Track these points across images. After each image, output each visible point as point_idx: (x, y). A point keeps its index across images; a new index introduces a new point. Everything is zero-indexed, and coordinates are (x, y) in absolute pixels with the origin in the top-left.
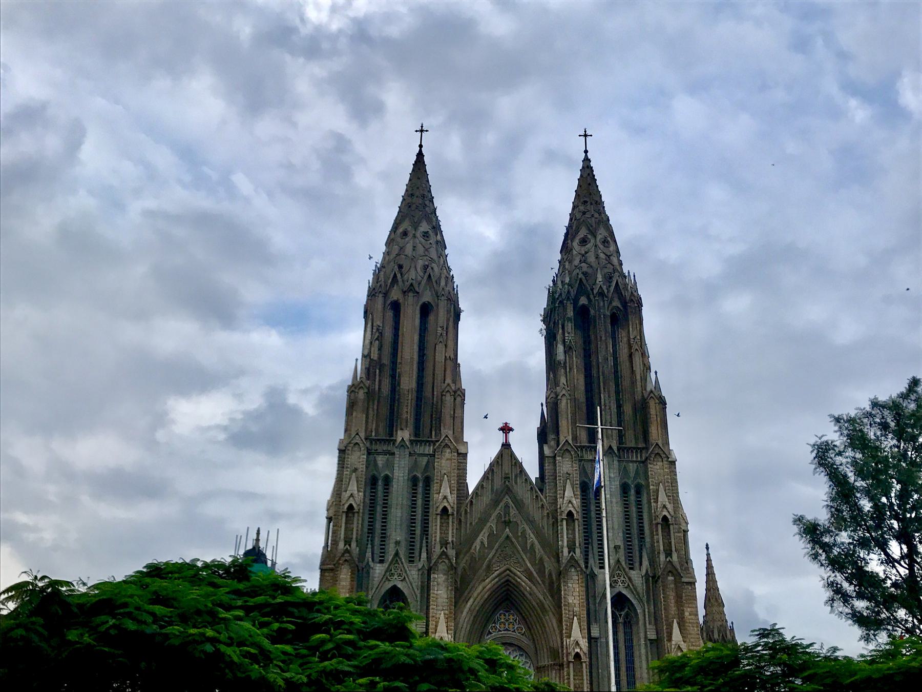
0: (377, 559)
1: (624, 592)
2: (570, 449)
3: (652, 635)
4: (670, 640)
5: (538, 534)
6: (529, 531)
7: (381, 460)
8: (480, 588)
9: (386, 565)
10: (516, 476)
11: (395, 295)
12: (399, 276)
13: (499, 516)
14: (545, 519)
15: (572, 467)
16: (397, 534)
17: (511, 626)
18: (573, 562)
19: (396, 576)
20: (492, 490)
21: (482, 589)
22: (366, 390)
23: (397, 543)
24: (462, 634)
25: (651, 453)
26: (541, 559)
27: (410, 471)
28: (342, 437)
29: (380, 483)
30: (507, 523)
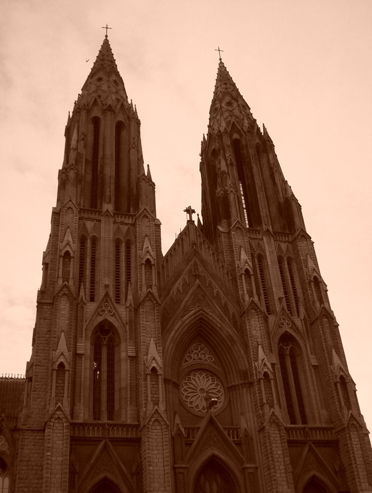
0: (88, 298)
1: (290, 331)
2: (241, 227)
3: (314, 362)
4: (331, 363)
7: (89, 225)
8: (180, 324)
10: (201, 243)
11: (96, 112)
12: (99, 101)
13: (190, 271)
14: (226, 275)
15: (243, 239)
16: (105, 280)
17: (203, 356)
20: (183, 253)
21: (182, 323)
22: (76, 171)
23: (107, 286)
25: (298, 235)
26: (226, 304)
27: (115, 234)
28: (55, 206)
29: (89, 241)
30: (197, 276)
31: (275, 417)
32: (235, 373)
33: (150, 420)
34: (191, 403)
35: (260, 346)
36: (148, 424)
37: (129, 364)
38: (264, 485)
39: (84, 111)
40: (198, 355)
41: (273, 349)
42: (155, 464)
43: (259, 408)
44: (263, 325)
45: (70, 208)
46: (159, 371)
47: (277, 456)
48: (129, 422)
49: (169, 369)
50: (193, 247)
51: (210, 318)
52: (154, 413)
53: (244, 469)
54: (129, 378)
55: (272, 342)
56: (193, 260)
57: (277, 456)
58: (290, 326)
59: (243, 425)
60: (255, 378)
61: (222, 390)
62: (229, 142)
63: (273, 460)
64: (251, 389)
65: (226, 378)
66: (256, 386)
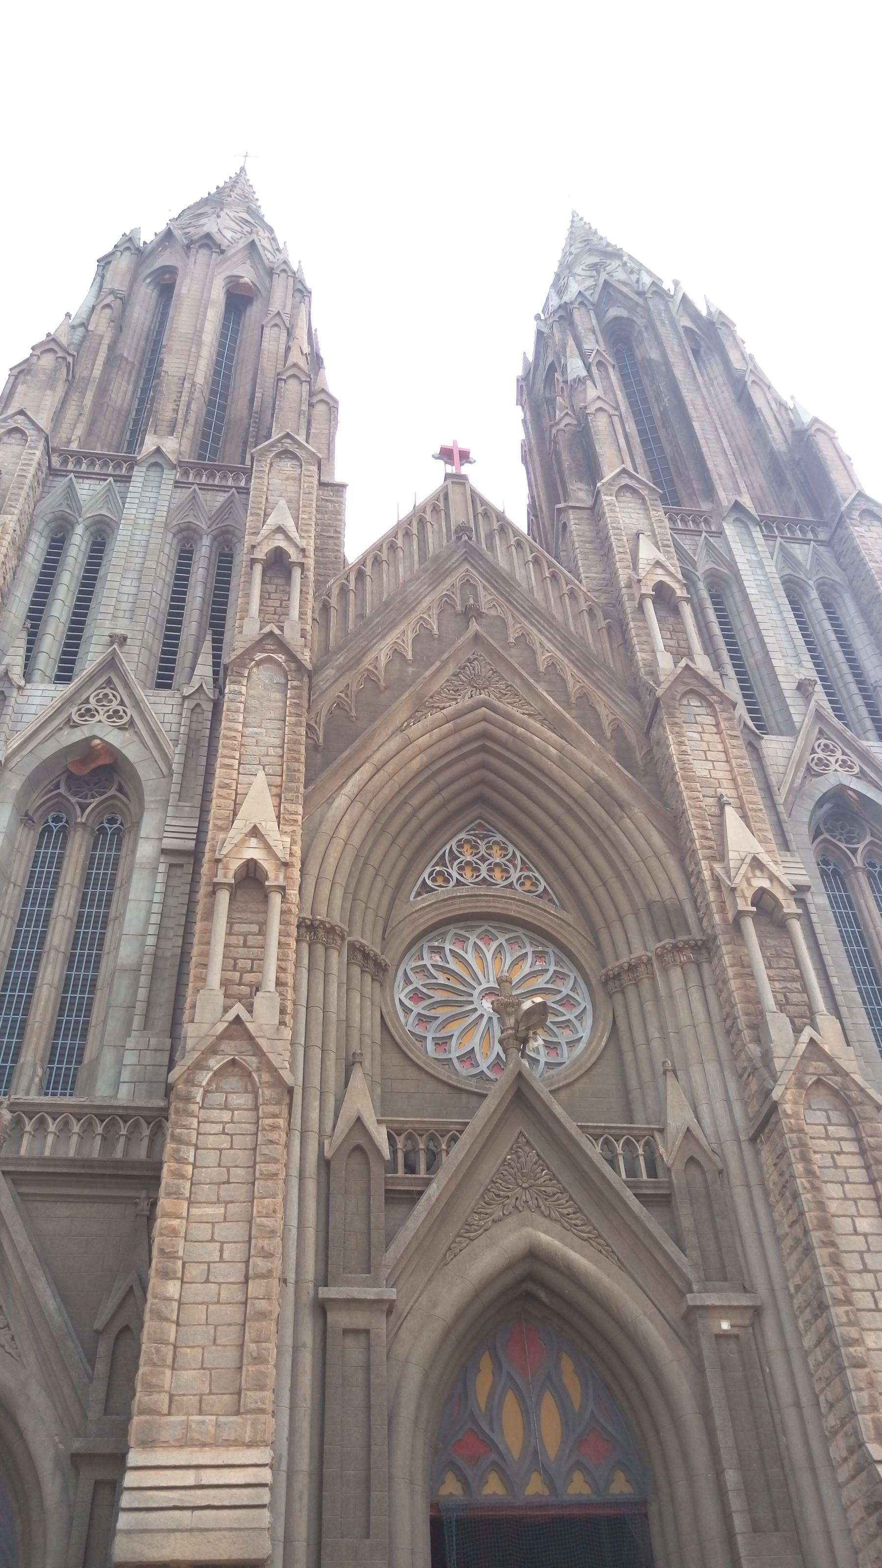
5: (567, 643)
6: (537, 637)
9: (71, 687)
10: (490, 536)
13: (446, 602)
17: (497, 874)
18: (694, 686)
19: (102, 716)
21: (402, 745)
24: (332, 861)
26: (584, 696)
29: (79, 529)
30: (471, 613)
31: (822, 1066)
32: (630, 920)
33: (199, 1066)
34: (442, 1043)
35: (728, 809)
36: (190, 1081)
37: (160, 878)
38: (805, 1399)
39: (127, 254)
40: (477, 869)
41: (790, 837)
42: (195, 1272)
43: (746, 1034)
44: (734, 742)
45: (16, 430)
46: (271, 875)
47: (858, 1243)
48: (124, 1096)
49: (339, 892)
50: (459, 538)
51: (520, 730)
52: (225, 1036)
53: (691, 1315)
54: (152, 929)
55: (784, 817)
56: (461, 572)
57: (858, 1243)
58: (856, 770)
59: (678, 1117)
60: (717, 918)
61: (583, 1000)
62: (594, 322)
63: (836, 1261)
64: (706, 967)
65: (598, 947)
66: (724, 949)
